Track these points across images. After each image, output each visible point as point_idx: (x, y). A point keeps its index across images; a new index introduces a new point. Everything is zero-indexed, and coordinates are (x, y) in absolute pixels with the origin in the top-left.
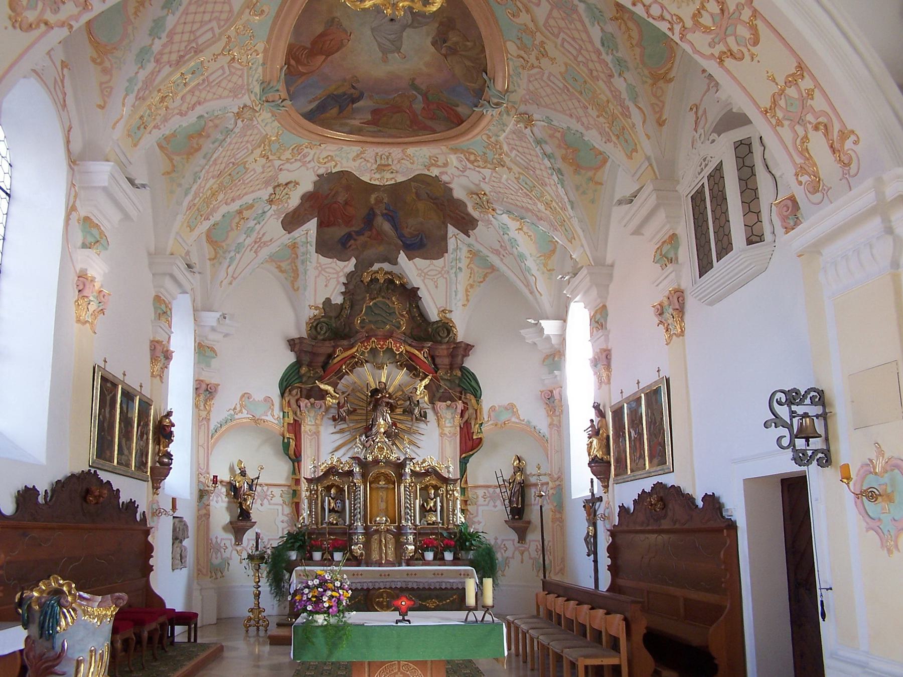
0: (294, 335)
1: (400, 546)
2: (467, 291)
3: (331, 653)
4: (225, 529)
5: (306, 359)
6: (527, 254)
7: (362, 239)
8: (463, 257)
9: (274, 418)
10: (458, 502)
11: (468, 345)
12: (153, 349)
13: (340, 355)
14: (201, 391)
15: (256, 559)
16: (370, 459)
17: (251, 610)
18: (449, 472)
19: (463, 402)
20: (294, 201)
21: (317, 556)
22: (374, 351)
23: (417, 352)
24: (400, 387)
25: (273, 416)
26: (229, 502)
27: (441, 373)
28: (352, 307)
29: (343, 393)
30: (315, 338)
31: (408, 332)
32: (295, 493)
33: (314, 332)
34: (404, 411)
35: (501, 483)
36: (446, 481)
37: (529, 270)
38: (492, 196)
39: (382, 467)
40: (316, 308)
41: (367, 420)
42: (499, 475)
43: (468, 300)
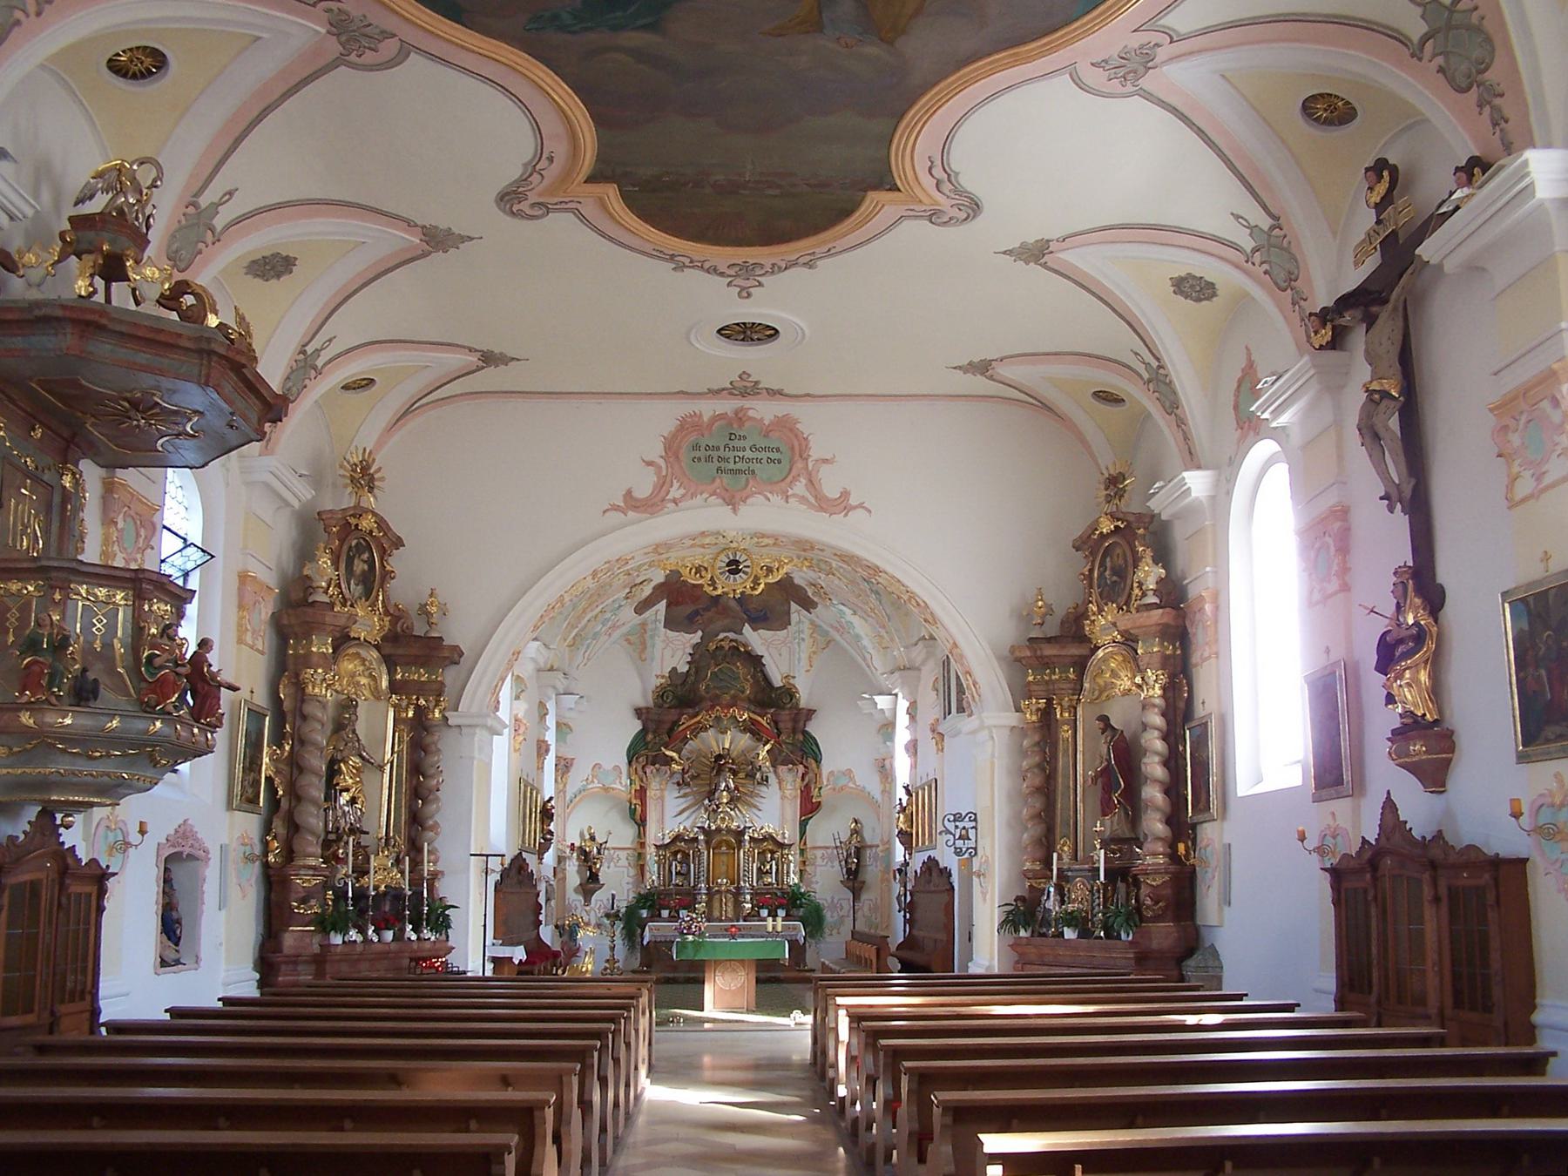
0: (641, 703)
1: (738, 904)
2: (810, 657)
3: (695, 955)
4: (576, 891)
5: (652, 726)
6: (862, 634)
7: (708, 615)
8: (806, 630)
9: (622, 785)
10: (792, 865)
11: (810, 710)
12: (539, 748)
13: (686, 722)
14: (559, 767)
15: (613, 916)
16: (713, 828)
17: (607, 961)
18: (784, 838)
19: (805, 767)
20: (647, 590)
21: (665, 913)
22: (718, 719)
23: (759, 719)
24: (743, 753)
25: (621, 783)
26: (579, 866)
27: (783, 737)
28: (696, 672)
29: (688, 759)
30: (660, 707)
31: (752, 697)
32: (640, 856)
33: (660, 700)
34: (747, 775)
35: (838, 844)
36: (782, 846)
37: (865, 647)
38: (828, 590)
39: (724, 835)
40: (663, 677)
41: (710, 785)
42: (837, 837)
43: (811, 666)
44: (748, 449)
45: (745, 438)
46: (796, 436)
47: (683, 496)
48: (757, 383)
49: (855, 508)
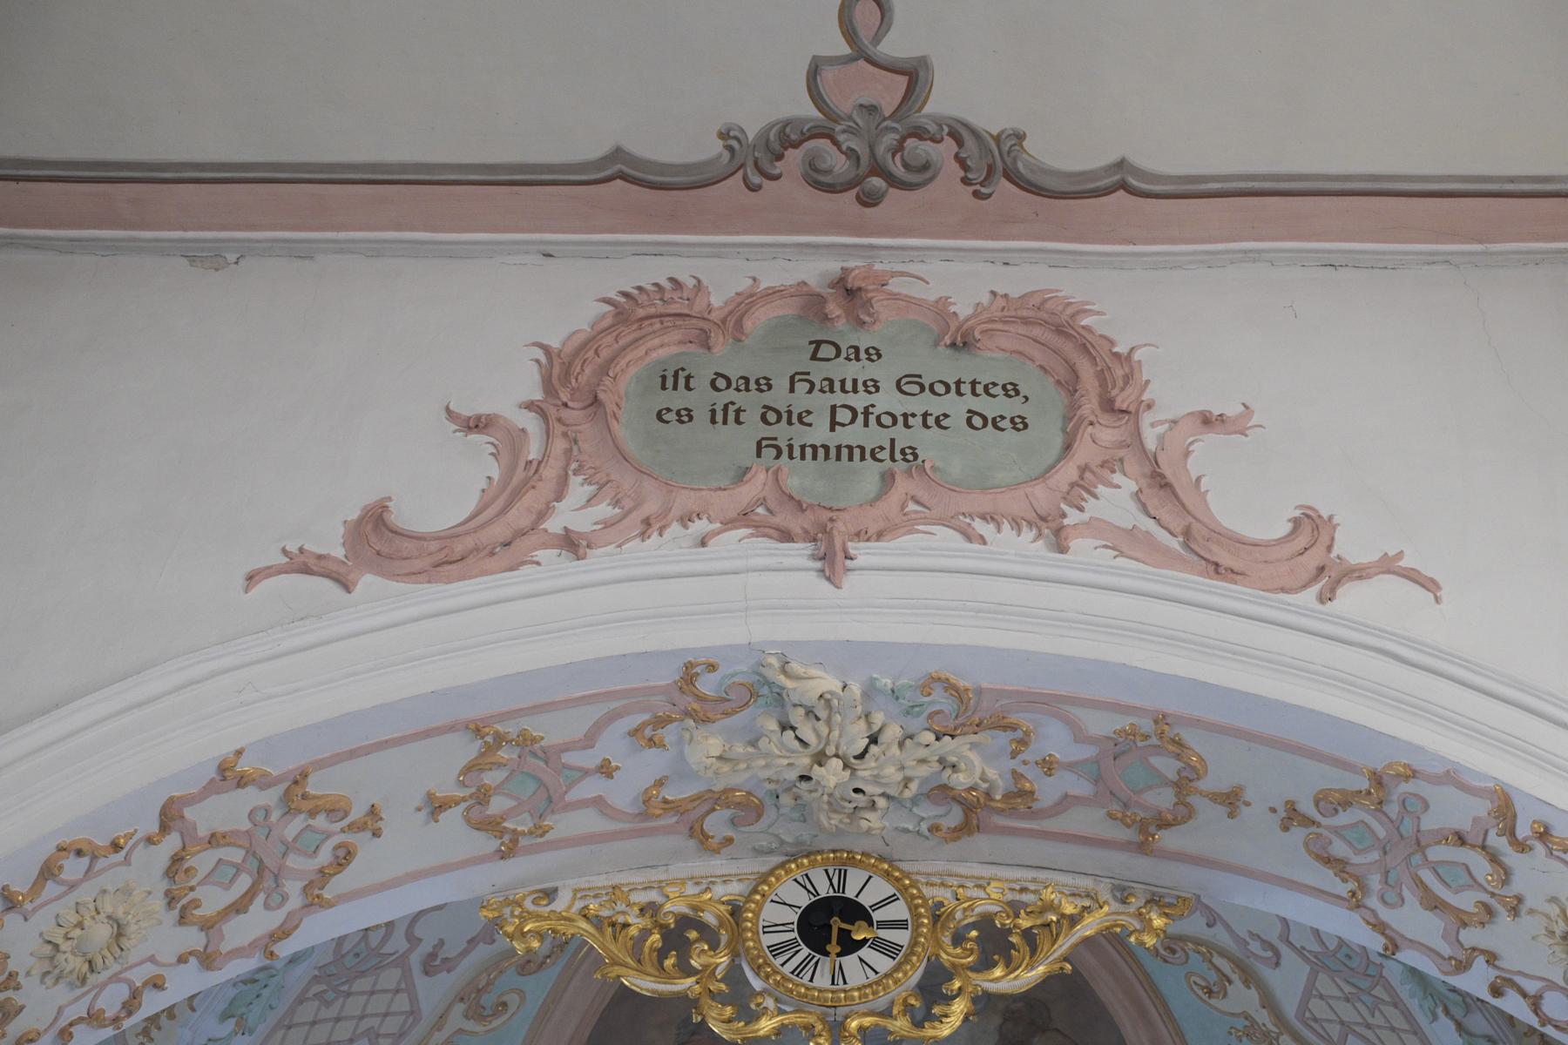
44: (887, 385)
45: (874, 354)
46: (1085, 349)
47: (608, 524)
48: (914, 75)
49: (1358, 573)
